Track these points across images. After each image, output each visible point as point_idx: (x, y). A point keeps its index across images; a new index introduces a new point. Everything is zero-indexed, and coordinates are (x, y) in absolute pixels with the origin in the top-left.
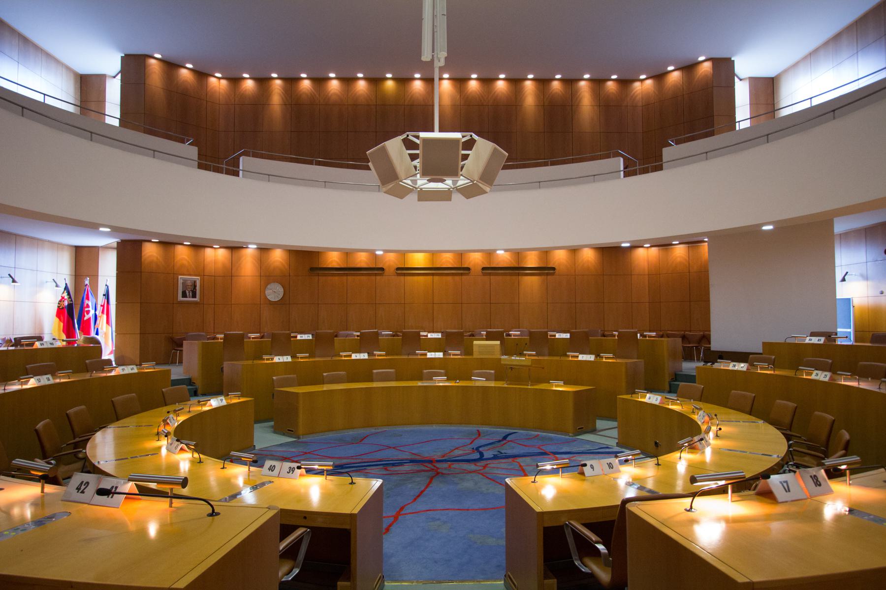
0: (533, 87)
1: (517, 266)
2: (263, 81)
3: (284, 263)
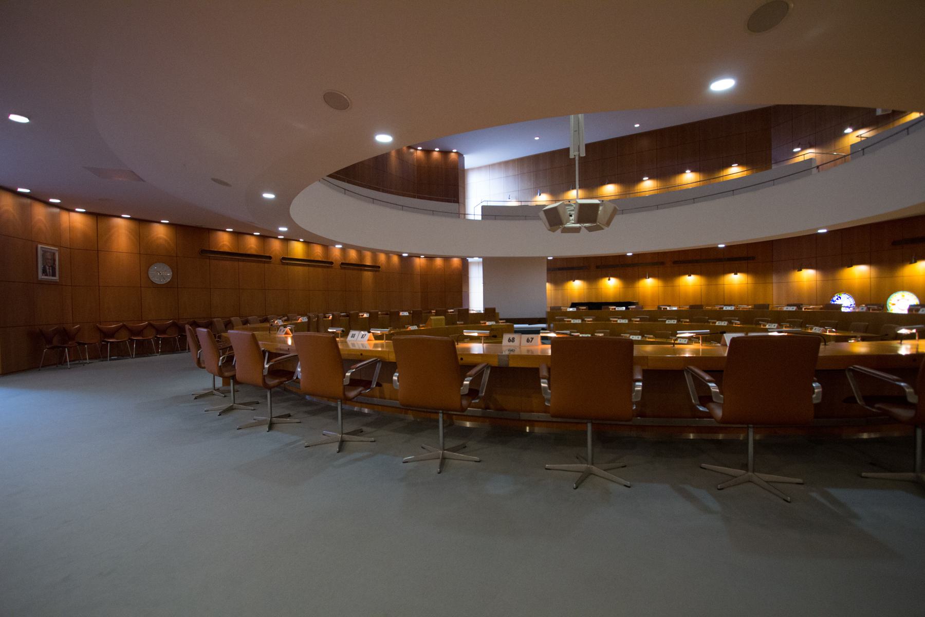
1: (360, 263)
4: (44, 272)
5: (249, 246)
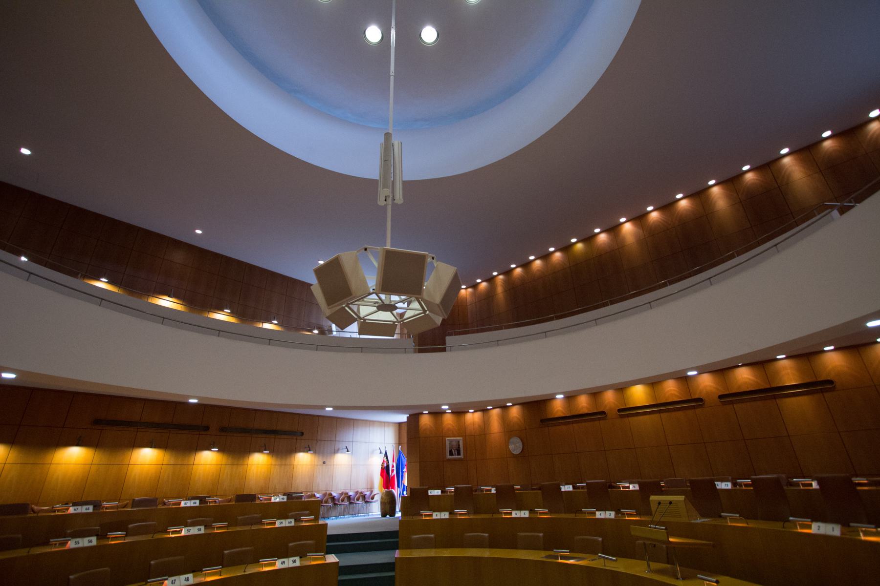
0: (722, 190)
2: (491, 280)
3: (519, 417)
4: (451, 454)
5: (580, 406)
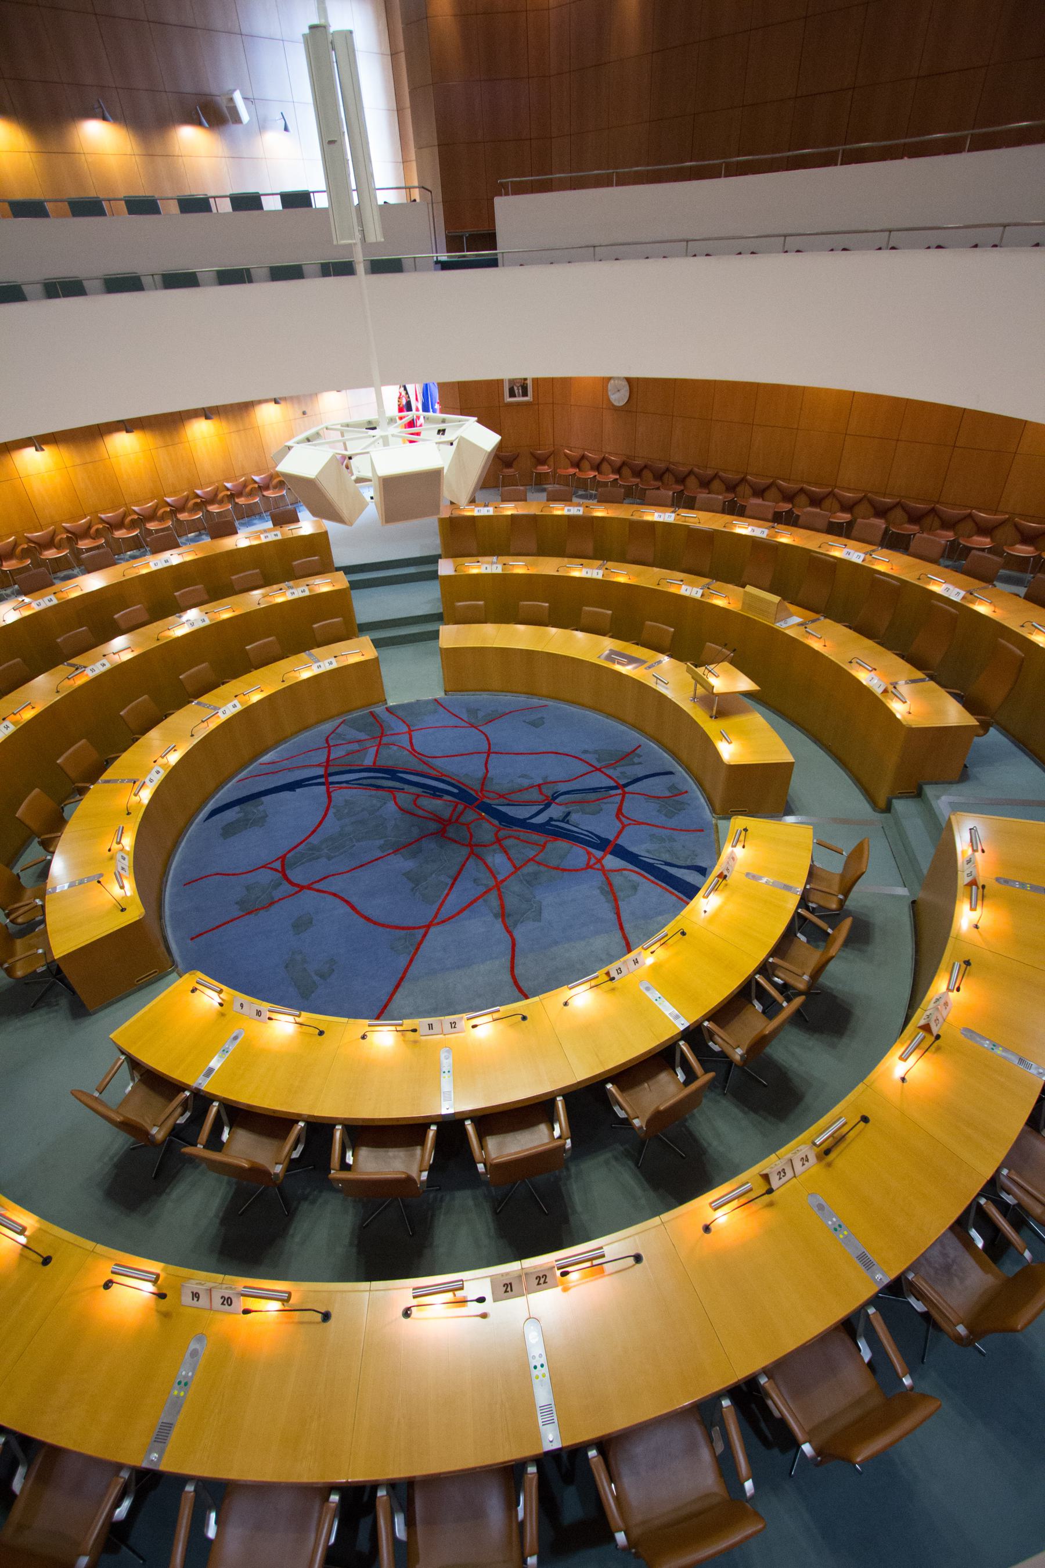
4: (512, 394)
